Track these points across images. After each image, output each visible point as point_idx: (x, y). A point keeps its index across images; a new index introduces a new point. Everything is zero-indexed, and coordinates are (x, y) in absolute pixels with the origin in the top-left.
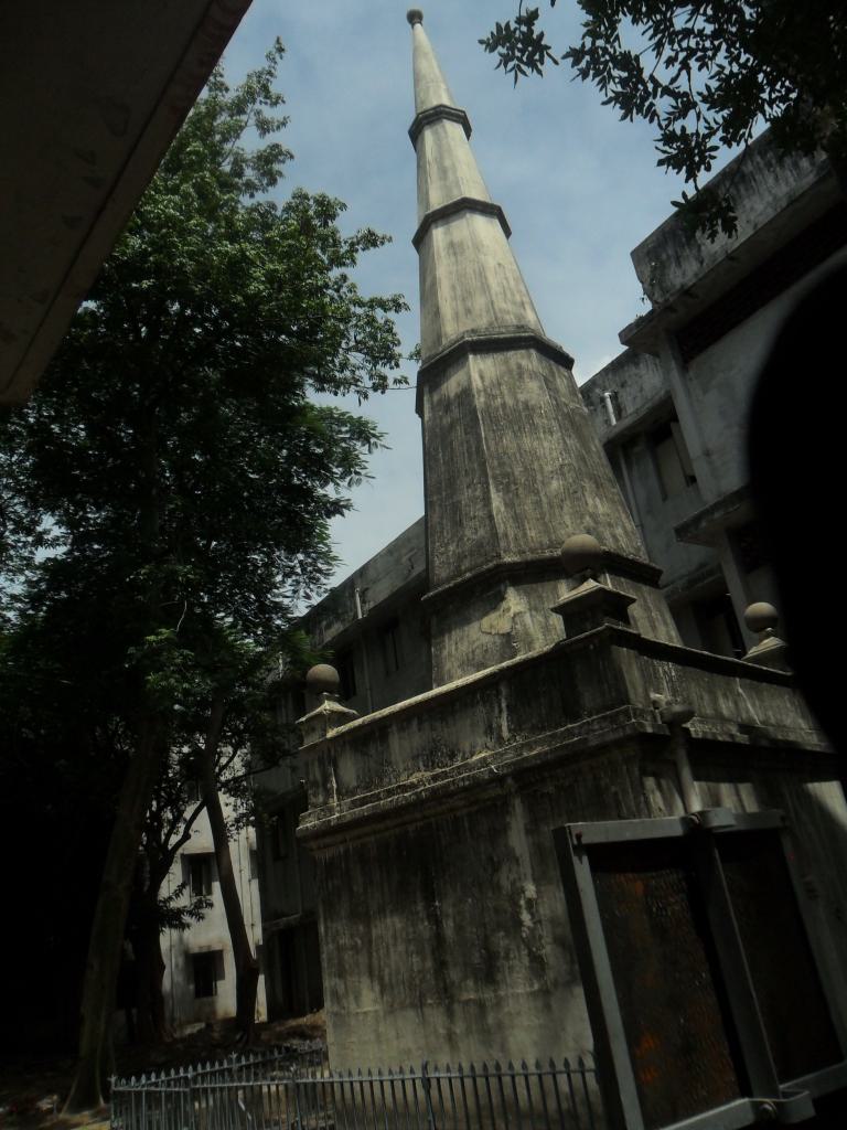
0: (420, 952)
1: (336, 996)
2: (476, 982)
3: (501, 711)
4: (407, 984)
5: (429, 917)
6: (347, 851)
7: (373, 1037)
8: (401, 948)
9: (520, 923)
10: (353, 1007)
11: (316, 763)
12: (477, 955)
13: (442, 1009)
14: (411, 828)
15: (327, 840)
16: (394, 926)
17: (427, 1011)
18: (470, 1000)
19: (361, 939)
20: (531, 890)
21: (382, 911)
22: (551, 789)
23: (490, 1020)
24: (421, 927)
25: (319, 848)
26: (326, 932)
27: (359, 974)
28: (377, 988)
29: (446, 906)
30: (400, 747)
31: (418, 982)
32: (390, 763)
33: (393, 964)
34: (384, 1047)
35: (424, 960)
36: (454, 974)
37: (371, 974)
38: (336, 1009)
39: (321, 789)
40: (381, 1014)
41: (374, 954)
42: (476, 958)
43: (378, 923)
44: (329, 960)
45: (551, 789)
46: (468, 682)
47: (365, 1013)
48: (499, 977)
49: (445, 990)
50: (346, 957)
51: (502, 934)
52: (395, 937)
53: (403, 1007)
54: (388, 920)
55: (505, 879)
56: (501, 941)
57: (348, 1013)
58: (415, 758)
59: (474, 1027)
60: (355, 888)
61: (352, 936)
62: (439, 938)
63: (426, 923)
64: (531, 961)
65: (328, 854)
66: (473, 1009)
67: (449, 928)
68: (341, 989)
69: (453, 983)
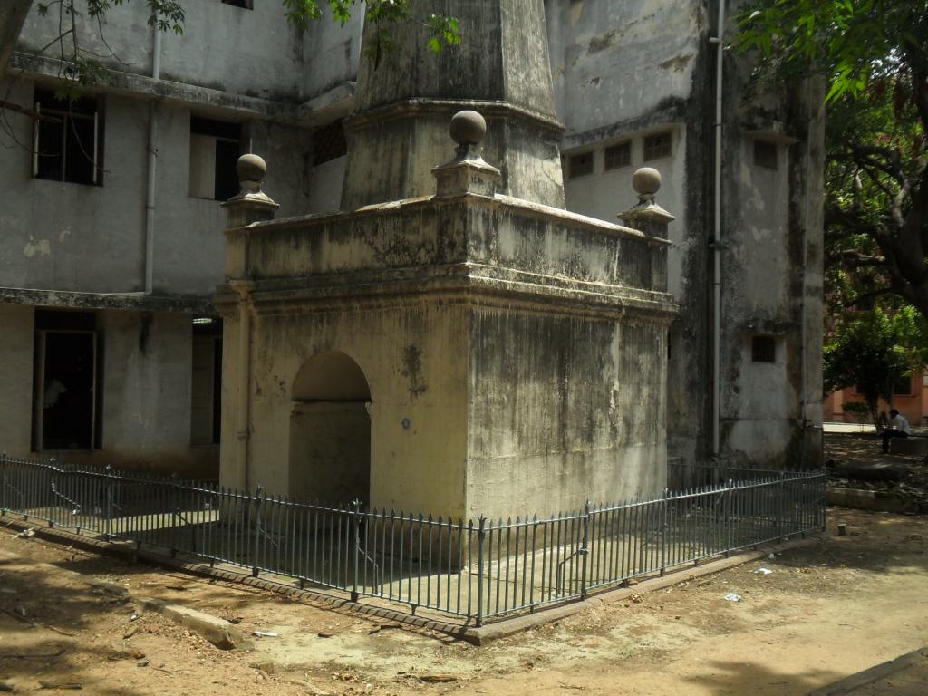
0: (551, 415)
1: (480, 443)
2: (582, 441)
3: (615, 259)
4: (539, 438)
5: (560, 389)
6: (504, 316)
7: (508, 478)
8: (538, 410)
9: (609, 405)
10: (494, 454)
11: (481, 217)
12: (585, 422)
13: (560, 458)
14: (556, 316)
15: (491, 300)
16: (534, 390)
17: (550, 458)
18: (577, 452)
19: (508, 396)
20: (617, 386)
21: (527, 376)
22: (634, 325)
23: (587, 466)
24: (554, 396)
25: (482, 304)
26: (477, 385)
27: (503, 426)
28: (516, 439)
29: (572, 384)
30: (555, 246)
31: (546, 437)
32: (542, 255)
33: (530, 421)
34: (516, 486)
35: (552, 421)
36: (570, 434)
37: (513, 428)
38: (479, 454)
39: (483, 246)
40: (517, 460)
41: (517, 411)
42: (585, 423)
43: (523, 385)
44: (478, 410)
45: (634, 325)
46: (545, 211)
47: (504, 458)
48: (594, 438)
49: (564, 443)
50: (493, 410)
51: (599, 410)
52: (534, 400)
53: (534, 456)
54: (531, 386)
55: (606, 373)
56: (599, 415)
57: (490, 458)
58: (561, 261)
59: (577, 471)
60: (507, 351)
61: (500, 392)
62: (564, 406)
63: (558, 394)
64: (611, 430)
65: (486, 312)
66: (578, 458)
67: (571, 398)
68: (486, 438)
69: (569, 440)
